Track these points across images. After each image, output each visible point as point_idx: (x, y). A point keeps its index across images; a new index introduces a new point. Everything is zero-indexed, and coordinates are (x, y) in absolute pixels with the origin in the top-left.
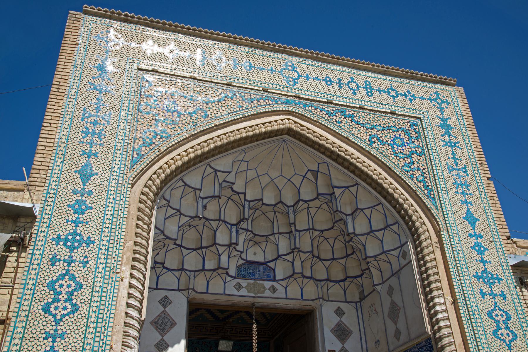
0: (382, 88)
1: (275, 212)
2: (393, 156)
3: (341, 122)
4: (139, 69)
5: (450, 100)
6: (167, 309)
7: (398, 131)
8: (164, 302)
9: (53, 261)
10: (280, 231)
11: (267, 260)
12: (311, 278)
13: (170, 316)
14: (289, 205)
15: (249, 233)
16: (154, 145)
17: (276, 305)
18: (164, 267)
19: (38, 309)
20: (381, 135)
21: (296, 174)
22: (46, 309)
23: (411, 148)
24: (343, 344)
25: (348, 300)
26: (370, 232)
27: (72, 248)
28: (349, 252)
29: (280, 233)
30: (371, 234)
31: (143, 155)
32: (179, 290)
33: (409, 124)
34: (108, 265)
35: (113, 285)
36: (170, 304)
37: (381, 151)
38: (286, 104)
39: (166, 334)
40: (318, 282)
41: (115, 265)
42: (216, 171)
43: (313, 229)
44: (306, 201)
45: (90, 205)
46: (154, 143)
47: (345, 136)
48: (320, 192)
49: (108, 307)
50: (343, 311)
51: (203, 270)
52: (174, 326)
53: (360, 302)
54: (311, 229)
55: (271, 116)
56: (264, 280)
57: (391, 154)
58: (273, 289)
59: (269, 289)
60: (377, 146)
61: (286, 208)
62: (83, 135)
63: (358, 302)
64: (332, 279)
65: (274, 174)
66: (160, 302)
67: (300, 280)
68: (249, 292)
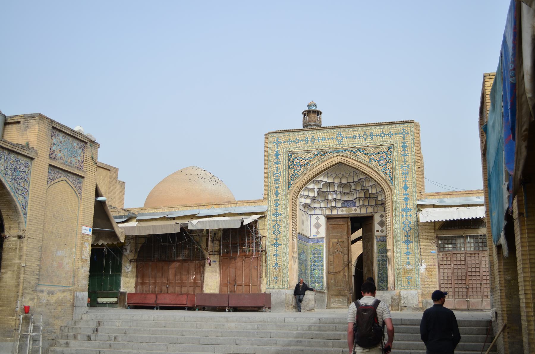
0: (378, 134)
5: (409, 132)
9: (273, 221)
19: (272, 233)
22: (274, 233)
27: (277, 217)
58: (356, 210)
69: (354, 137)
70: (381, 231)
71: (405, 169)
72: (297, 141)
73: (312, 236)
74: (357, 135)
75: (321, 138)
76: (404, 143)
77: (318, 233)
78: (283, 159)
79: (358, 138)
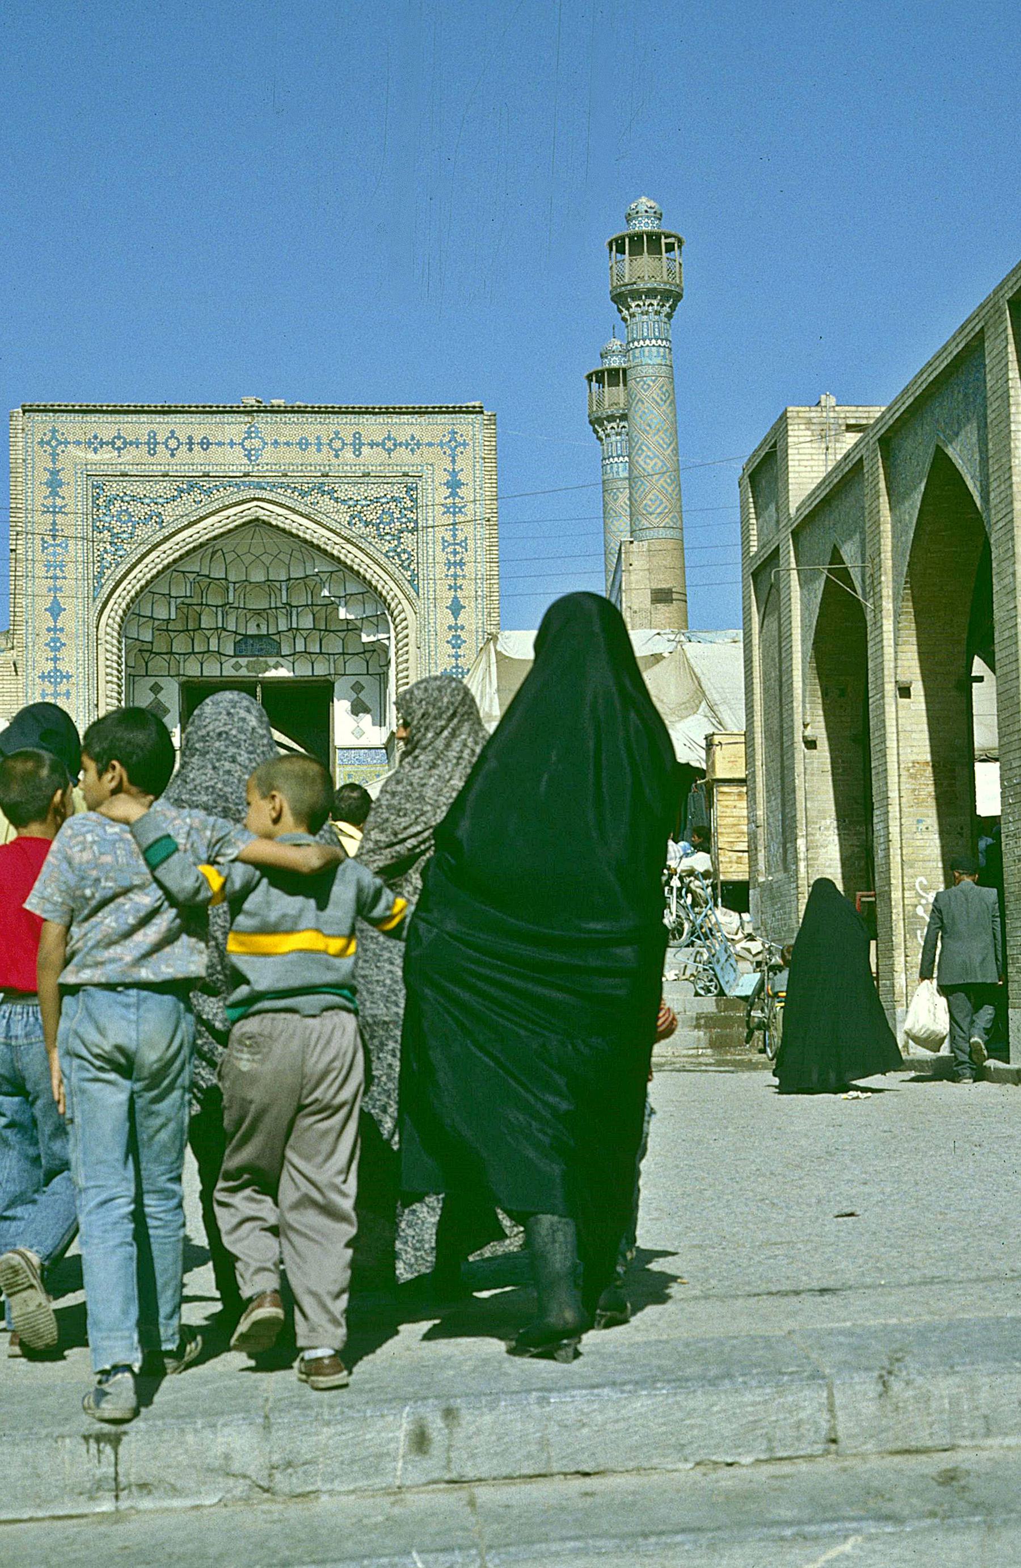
12: (321, 653)
27: (56, 684)
42: (183, 572)
43: (312, 605)
51: (193, 653)
69: (300, 444)
71: (455, 553)
72: (119, 443)
74: (312, 440)
75: (197, 439)
76: (454, 473)
78: (74, 495)
79: (314, 448)
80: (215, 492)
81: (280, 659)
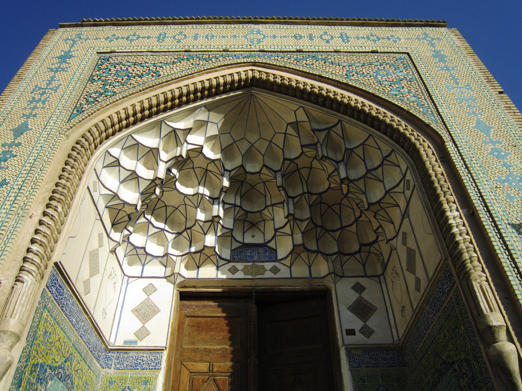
1: (264, 182)
2: (376, 84)
3: (313, 64)
4: (98, 53)
6: (151, 297)
7: (381, 65)
8: (149, 289)
10: (273, 203)
11: (266, 241)
12: (318, 252)
13: (153, 303)
14: (276, 169)
15: (237, 209)
16: (96, 103)
17: (282, 287)
18: (147, 254)
20: (361, 69)
21: (276, 133)
23: (398, 76)
24: (365, 322)
25: (368, 274)
26: (366, 174)
28: (358, 214)
29: (273, 205)
30: (369, 175)
31: (84, 111)
32: (165, 277)
33: (395, 59)
34: (16, 202)
35: (17, 221)
36: (154, 291)
37: (362, 82)
38: (249, 57)
39: (147, 321)
40: (328, 257)
41: (25, 203)
44: (292, 160)
45: (15, 154)
46: (97, 101)
47: (317, 74)
48: (303, 144)
49: (5, 242)
50: (362, 286)
52: (157, 313)
53: (383, 274)
54: (305, 193)
55: (232, 68)
56: (264, 262)
57: (374, 83)
59: (270, 270)
60: (357, 78)
61: (273, 173)
62: (29, 103)
63: (381, 275)
64: (345, 252)
65: (253, 138)
66: (145, 290)
67: (304, 255)
68: (245, 274)
70: (361, 331)
73: (119, 343)
77: (143, 333)
80: (214, 60)
81: (277, 264)
